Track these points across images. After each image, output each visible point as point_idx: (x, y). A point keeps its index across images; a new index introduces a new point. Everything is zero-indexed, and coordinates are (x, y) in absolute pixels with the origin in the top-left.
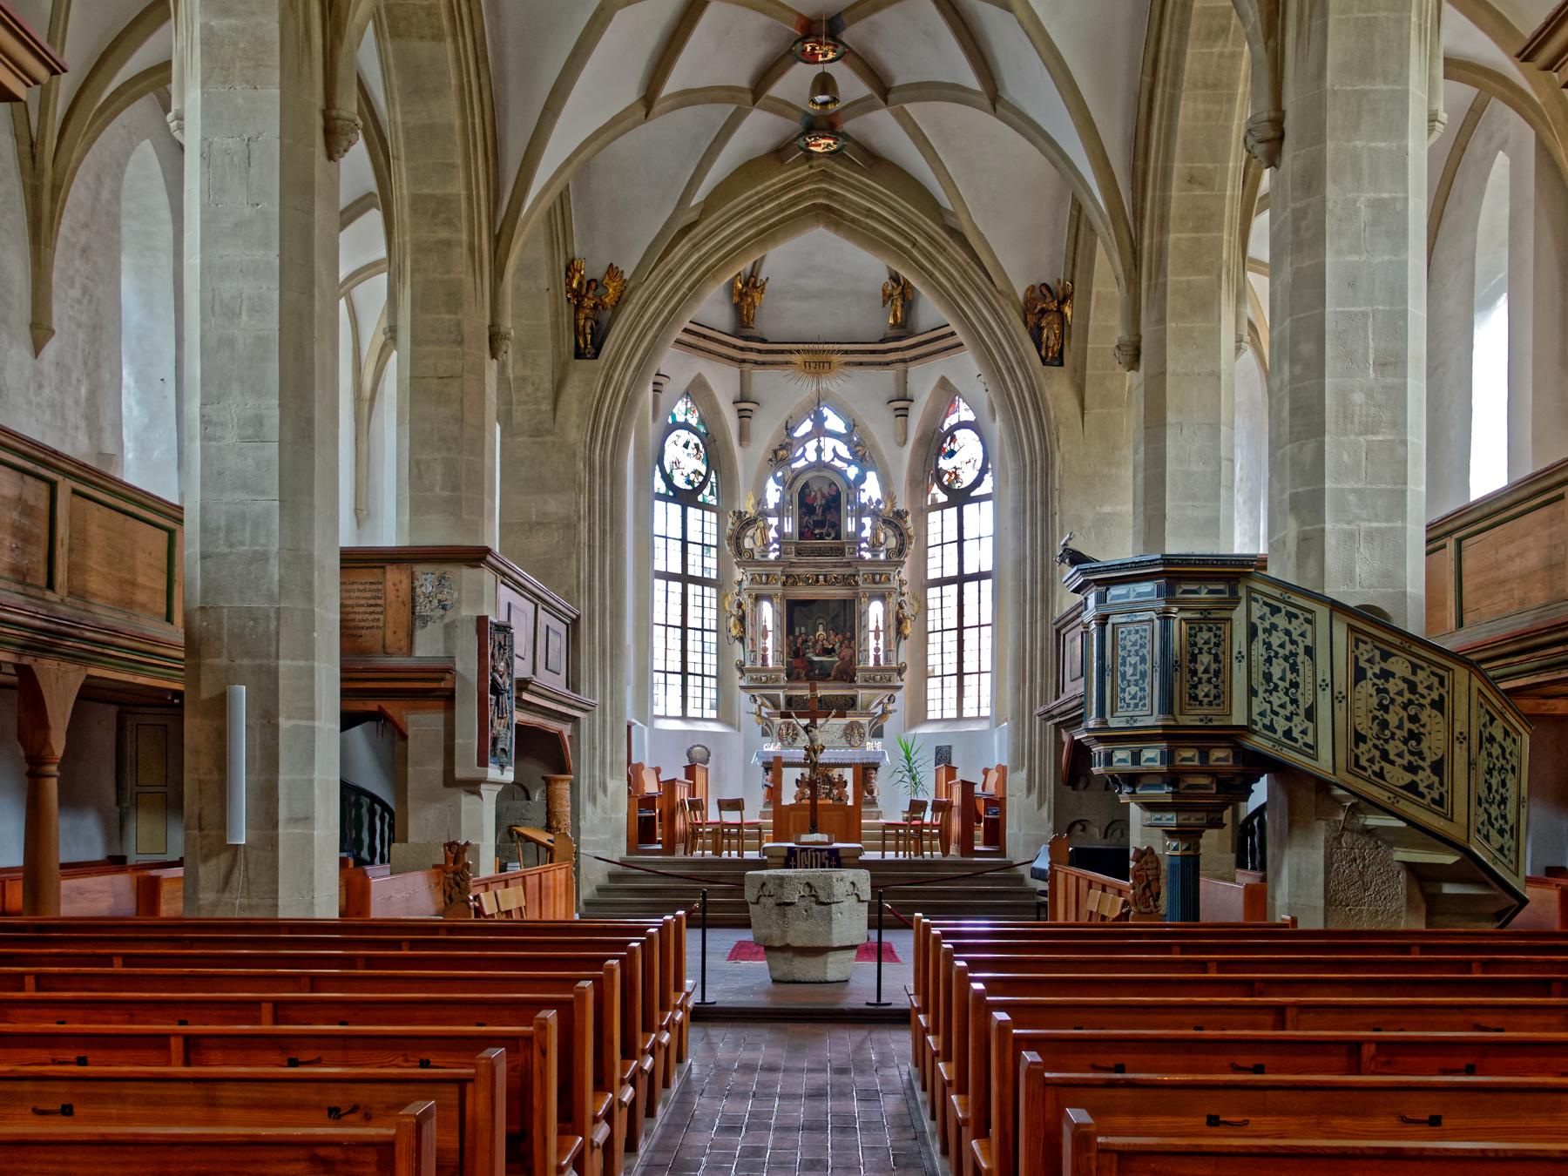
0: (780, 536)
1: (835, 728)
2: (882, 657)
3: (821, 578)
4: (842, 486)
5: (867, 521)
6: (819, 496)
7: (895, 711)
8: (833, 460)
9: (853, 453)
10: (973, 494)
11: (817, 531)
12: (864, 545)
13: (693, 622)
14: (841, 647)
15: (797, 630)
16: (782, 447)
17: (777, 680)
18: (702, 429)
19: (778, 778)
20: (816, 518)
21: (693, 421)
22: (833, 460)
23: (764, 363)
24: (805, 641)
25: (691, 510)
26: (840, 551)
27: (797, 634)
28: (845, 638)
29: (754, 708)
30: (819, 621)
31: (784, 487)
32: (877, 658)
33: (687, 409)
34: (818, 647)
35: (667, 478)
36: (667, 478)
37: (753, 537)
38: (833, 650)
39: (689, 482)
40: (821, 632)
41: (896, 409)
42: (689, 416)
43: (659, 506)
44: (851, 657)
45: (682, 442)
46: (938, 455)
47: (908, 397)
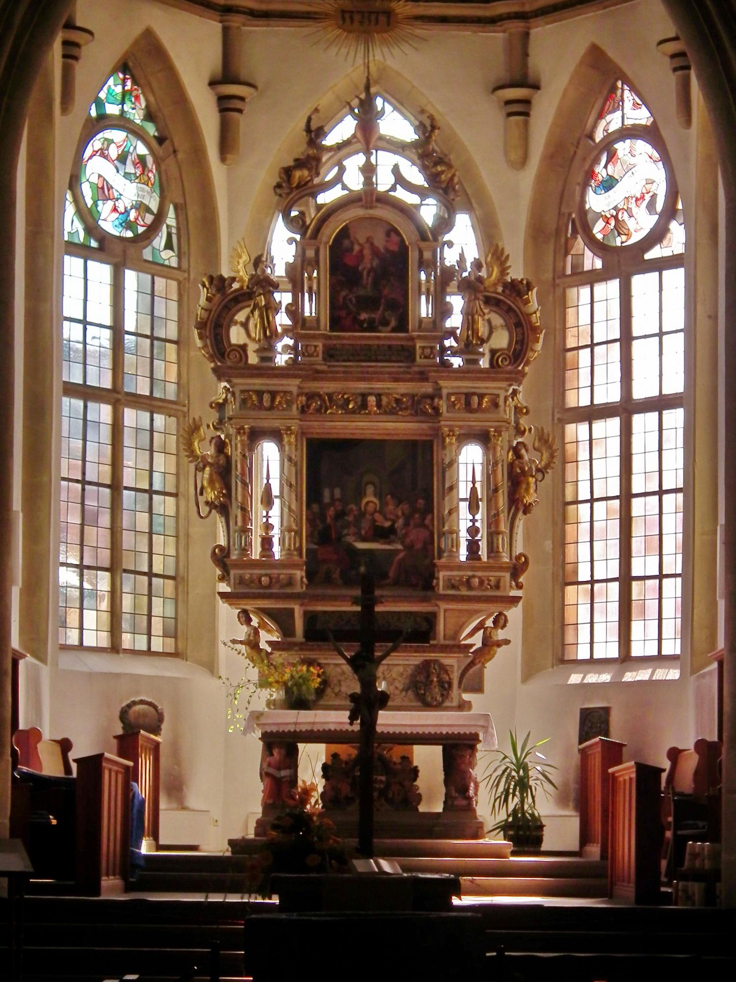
2: (483, 546)
3: (372, 400)
4: (409, 235)
5: (457, 302)
6: (367, 252)
7: (507, 642)
8: (394, 188)
9: (433, 178)
11: (364, 316)
12: (449, 342)
13: (129, 478)
14: (406, 524)
15: (327, 493)
16: (300, 163)
17: (290, 582)
18: (151, 130)
19: (291, 758)
20: (361, 292)
21: (136, 116)
22: (394, 188)
24: (340, 515)
25: (131, 277)
26: (406, 354)
27: (327, 499)
29: (242, 631)
30: (366, 479)
31: (303, 235)
32: (473, 547)
33: (124, 93)
34: (365, 525)
35: (88, 217)
36: (88, 217)
38: (392, 530)
39: (128, 225)
40: (370, 498)
41: (508, 102)
42: (127, 107)
43: (72, 265)
44: (425, 544)
45: (113, 152)
47: (531, 81)
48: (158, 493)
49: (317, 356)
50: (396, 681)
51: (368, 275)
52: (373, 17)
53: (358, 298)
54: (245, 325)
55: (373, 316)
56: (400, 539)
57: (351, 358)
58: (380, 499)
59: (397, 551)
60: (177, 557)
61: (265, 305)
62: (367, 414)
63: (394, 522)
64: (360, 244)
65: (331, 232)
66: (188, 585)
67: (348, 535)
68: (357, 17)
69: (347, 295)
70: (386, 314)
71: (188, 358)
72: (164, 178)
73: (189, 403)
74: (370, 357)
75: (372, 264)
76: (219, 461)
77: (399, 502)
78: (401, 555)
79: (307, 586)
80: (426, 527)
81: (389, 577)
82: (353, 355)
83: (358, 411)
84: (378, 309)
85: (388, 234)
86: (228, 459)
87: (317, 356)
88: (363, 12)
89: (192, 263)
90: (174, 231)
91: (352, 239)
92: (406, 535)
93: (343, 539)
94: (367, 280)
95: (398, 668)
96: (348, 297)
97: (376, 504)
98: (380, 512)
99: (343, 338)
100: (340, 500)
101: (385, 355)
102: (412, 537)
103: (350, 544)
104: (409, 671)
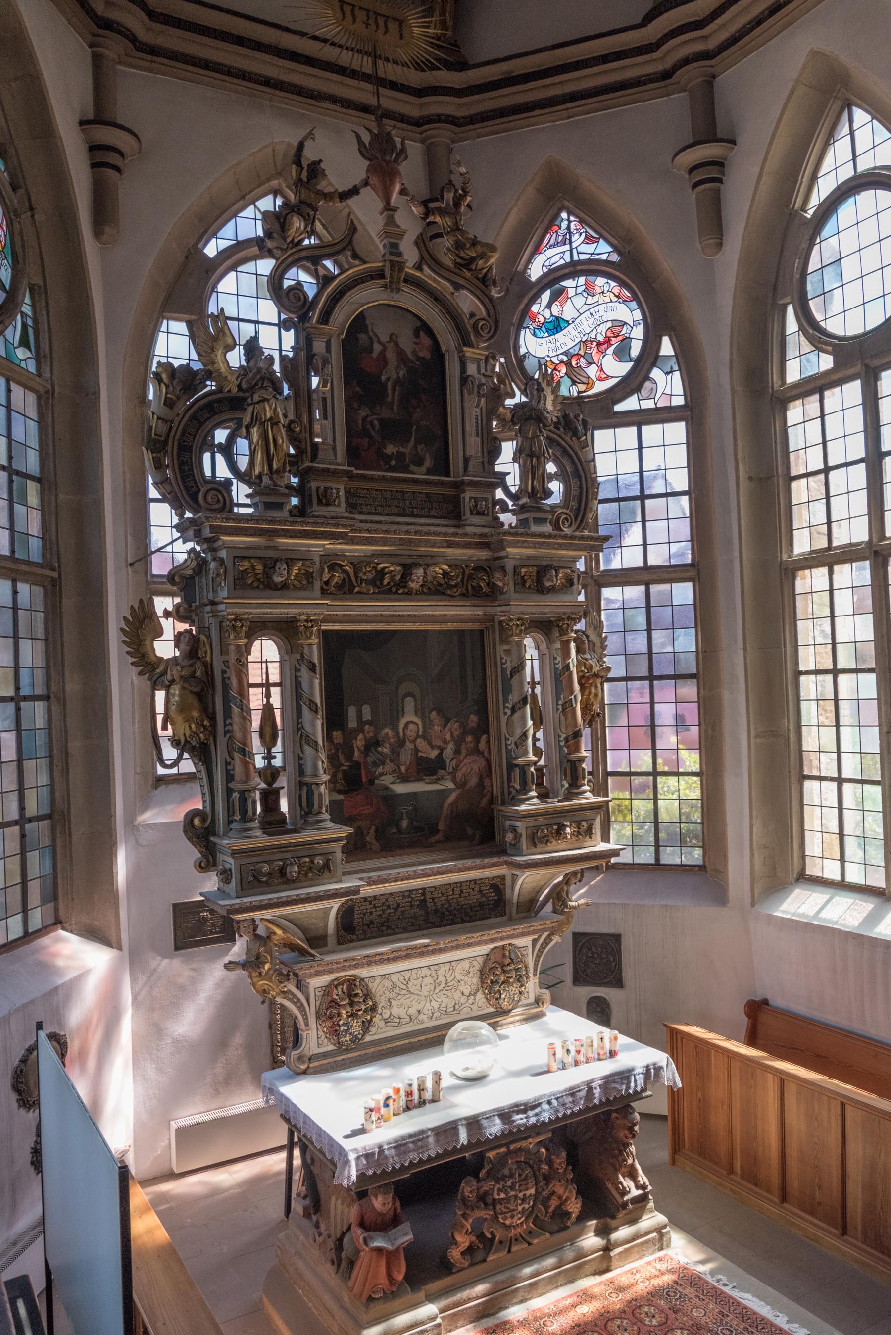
0: (300, 451)
1: (459, 968)
6: (390, 355)
10: (618, 408)
11: (390, 449)
14: (457, 752)
15: (352, 712)
20: (385, 414)
23: (153, 51)
24: (373, 744)
27: (353, 724)
28: (465, 733)
30: (402, 690)
34: (406, 757)
37: (227, 450)
38: (440, 762)
44: (481, 778)
46: (520, 326)
48: (26, 698)
49: (339, 505)
50: (462, 983)
51: (394, 390)
52: (381, 21)
53: (382, 422)
54: (227, 450)
55: (402, 449)
57: (380, 510)
58: (423, 718)
59: (449, 792)
60: (52, 786)
61: (271, 419)
62: (407, 594)
63: (442, 750)
64: (379, 342)
65: (343, 315)
66: (70, 822)
67: (382, 775)
68: (361, 15)
69: (367, 416)
70: (419, 447)
71: (56, 503)
72: (17, 238)
73: (59, 567)
74: (404, 510)
75: (398, 374)
76: (194, 672)
77: (448, 721)
78: (453, 797)
80: (482, 753)
81: (438, 831)
82: (382, 506)
83: (394, 590)
84: (409, 441)
85: (416, 334)
86: (209, 669)
87: (339, 505)
88: (368, 11)
89: (55, 371)
90: (30, 322)
91: (371, 334)
92: (455, 769)
93: (376, 782)
94: (393, 396)
95: (463, 962)
96: (369, 419)
97: (417, 725)
98: (424, 737)
99: (371, 479)
100: (369, 723)
101: (423, 508)
103: (387, 788)
104: (477, 967)
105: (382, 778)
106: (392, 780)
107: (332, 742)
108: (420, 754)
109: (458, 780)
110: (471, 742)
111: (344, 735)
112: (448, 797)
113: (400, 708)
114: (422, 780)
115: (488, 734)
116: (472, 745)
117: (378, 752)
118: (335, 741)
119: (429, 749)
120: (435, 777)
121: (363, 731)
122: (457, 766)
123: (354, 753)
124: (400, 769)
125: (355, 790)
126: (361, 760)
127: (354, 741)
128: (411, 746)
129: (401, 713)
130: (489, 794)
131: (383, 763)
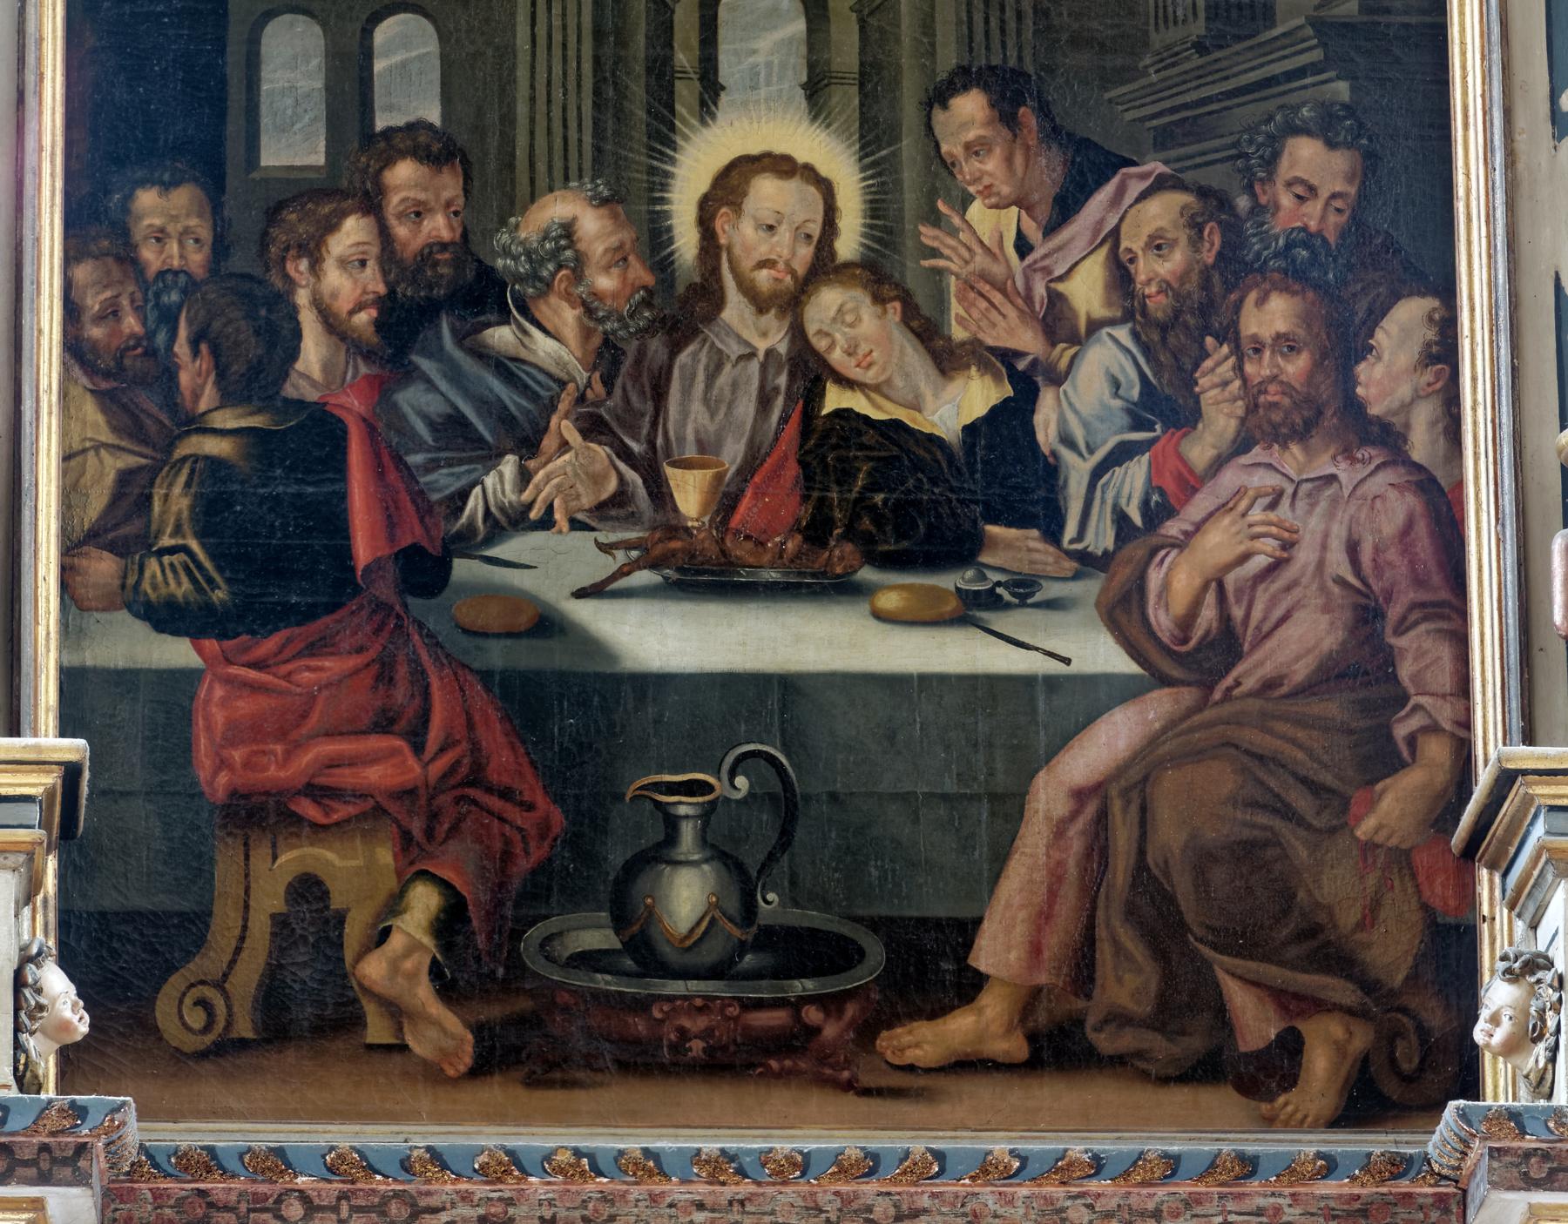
56: (1088, 562)
67: (516, 520)
79: (72, 1059)
81: (970, 986)
93: (462, 569)
97: (826, 188)
102: (1218, 543)
103: (547, 625)
105: (512, 548)
106: (600, 567)
107: (128, 259)
108: (835, 399)
109: (1162, 620)
110: (1287, 344)
111: (216, 207)
112: (1063, 740)
113: (684, 59)
114: (841, 589)
115: (1446, 289)
116: (1296, 367)
117: (482, 355)
118: (150, 255)
119: (915, 359)
120: (948, 581)
121: (372, 203)
122: (1157, 512)
123: (293, 353)
124: (660, 493)
125: (286, 615)
126: (352, 405)
127: (299, 268)
128: (772, 336)
129: (686, 93)
130: (1437, 751)
131: (529, 444)
